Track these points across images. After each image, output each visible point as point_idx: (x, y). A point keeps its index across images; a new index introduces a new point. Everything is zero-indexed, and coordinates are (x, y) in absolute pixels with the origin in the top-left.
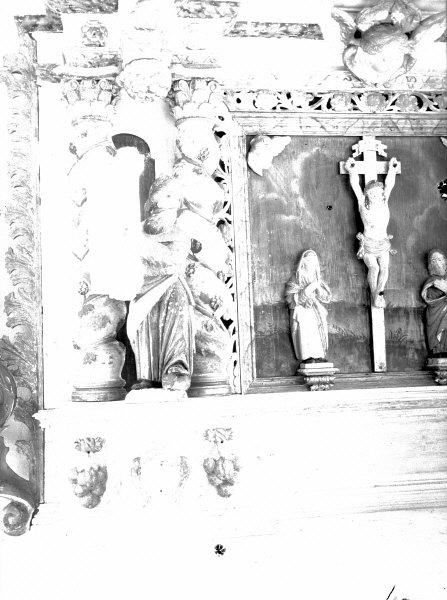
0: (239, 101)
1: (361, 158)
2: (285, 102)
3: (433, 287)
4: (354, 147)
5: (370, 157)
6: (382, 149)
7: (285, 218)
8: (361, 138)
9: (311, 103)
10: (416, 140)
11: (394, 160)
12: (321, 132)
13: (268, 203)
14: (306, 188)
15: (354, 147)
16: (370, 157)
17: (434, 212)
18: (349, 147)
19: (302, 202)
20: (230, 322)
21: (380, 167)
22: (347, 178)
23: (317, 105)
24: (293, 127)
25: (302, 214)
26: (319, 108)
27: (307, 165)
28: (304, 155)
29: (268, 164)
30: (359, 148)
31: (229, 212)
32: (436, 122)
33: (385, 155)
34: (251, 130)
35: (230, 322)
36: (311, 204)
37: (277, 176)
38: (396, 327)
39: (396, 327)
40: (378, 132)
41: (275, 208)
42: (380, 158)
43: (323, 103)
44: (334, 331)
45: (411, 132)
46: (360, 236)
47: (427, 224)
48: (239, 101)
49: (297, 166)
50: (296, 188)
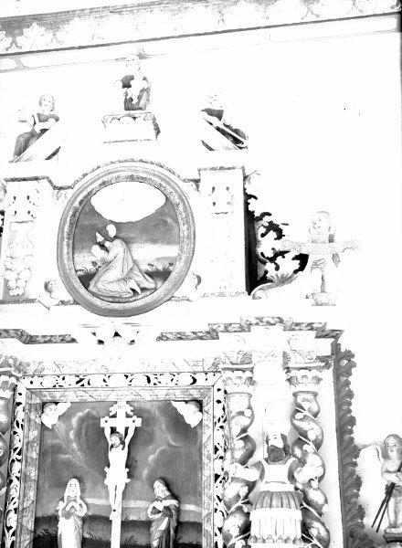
0: (32, 382)
1: (114, 416)
2: (61, 383)
3: (154, 508)
4: (111, 409)
5: (121, 415)
6: (129, 409)
7: (63, 456)
8: (116, 402)
9: (77, 383)
11: (135, 417)
12: (90, 399)
13: (53, 446)
14: (78, 434)
15: (111, 409)
16: (121, 415)
17: (163, 452)
19: (74, 445)
20: (11, 528)
21: (129, 422)
22: (103, 429)
23: (81, 384)
24: (72, 397)
25: (75, 453)
27: (82, 420)
29: (55, 421)
30: (113, 410)
31: (19, 454)
33: (131, 414)
34: (45, 399)
35: (11, 528)
36: (80, 450)
37: (62, 427)
38: (129, 535)
39: (129, 535)
40: (129, 399)
41: (57, 450)
42: (128, 416)
43: (85, 382)
44: (87, 536)
45: (150, 398)
47: (157, 461)
48: (32, 382)
49: (74, 421)
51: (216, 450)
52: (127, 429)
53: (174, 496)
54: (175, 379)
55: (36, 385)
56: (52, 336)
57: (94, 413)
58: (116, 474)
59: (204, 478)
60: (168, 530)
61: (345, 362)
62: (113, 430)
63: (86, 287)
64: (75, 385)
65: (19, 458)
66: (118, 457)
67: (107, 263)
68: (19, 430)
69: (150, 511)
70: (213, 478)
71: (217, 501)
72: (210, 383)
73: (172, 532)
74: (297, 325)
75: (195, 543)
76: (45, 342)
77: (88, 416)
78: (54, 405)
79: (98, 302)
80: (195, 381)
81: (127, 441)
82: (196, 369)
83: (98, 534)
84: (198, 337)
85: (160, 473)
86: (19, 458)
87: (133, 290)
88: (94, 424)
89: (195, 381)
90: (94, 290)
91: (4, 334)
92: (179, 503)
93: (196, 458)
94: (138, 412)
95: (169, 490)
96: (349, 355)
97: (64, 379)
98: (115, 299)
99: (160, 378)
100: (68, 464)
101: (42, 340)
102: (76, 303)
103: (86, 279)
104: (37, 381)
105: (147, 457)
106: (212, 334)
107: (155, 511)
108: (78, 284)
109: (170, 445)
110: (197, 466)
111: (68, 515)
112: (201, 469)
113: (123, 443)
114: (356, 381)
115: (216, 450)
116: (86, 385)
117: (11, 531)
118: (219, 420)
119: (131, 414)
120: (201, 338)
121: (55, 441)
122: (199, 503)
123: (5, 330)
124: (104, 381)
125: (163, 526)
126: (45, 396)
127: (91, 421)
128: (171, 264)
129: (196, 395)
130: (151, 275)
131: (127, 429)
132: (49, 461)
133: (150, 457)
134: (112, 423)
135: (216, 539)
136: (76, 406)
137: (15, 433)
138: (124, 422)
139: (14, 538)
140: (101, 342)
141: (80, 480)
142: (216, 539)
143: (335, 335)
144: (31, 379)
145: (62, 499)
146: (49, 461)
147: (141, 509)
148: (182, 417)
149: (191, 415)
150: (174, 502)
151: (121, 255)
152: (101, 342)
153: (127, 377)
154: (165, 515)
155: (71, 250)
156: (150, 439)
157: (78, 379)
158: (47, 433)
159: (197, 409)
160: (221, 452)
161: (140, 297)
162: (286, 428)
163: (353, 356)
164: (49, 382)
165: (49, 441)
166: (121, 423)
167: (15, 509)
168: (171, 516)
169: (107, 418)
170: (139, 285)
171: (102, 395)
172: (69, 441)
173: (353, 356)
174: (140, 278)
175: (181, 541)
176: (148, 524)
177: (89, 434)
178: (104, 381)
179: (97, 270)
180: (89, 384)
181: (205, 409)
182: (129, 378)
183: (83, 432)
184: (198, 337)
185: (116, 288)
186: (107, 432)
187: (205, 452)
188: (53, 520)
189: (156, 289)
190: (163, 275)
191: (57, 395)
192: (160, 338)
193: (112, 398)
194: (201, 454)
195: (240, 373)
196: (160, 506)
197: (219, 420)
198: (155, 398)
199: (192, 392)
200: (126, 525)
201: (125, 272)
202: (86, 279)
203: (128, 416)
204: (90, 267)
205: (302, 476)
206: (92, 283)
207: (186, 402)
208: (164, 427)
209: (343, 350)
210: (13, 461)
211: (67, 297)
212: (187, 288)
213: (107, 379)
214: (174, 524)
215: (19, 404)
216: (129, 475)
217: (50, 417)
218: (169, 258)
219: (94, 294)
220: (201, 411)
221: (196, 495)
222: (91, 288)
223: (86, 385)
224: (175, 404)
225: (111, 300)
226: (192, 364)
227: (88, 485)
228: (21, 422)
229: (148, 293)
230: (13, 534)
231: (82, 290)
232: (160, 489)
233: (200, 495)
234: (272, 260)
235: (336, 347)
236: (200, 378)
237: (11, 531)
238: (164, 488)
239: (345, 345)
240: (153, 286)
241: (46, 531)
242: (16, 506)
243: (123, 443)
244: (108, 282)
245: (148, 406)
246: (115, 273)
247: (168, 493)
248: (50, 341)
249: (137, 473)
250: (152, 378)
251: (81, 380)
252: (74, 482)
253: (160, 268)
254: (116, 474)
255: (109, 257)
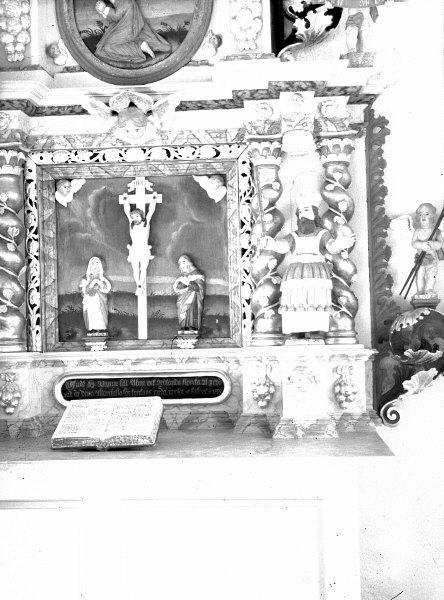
0: (41, 158)
1: (133, 193)
2: (74, 158)
3: (180, 283)
4: (129, 185)
5: (140, 191)
6: (148, 185)
7: (83, 235)
8: (134, 178)
9: (91, 158)
10: (175, 178)
11: (155, 194)
12: (106, 175)
14: (96, 212)
15: (129, 185)
16: (140, 191)
17: (186, 228)
18: (123, 183)
19: (93, 224)
20: (35, 305)
21: (149, 199)
22: (122, 206)
24: (87, 173)
25: (95, 232)
26: (98, 161)
27: (99, 198)
28: (96, 191)
29: (70, 198)
30: (131, 186)
31: (36, 233)
32: (186, 166)
33: (151, 190)
34: (57, 176)
35: (35, 305)
37: (78, 207)
39: (157, 309)
40: (147, 174)
41: (73, 229)
42: (147, 192)
43: (99, 157)
44: (113, 311)
46: (128, 246)
47: (181, 237)
48: (41, 158)
49: (91, 198)
50: (89, 213)
51: (243, 224)
52: (147, 206)
53: (200, 271)
54: (197, 152)
55: (47, 160)
56: (60, 107)
57: (111, 189)
58: (139, 251)
59: (230, 253)
60: (195, 303)
61: (377, 130)
62: (133, 208)
63: (93, 50)
64: (88, 161)
65: (36, 237)
66: (140, 234)
67: (114, 22)
68: (33, 209)
69: (175, 285)
70: (240, 252)
71: (245, 274)
72: (234, 155)
73: (199, 305)
74: (330, 89)
75: (222, 314)
76: (53, 114)
77: (105, 193)
78: (67, 184)
79: (104, 66)
80: (218, 154)
81: (149, 218)
82: (219, 141)
83: (124, 308)
84: (221, 105)
85: (184, 249)
86: (36, 237)
87: (146, 54)
88: (112, 202)
89: (218, 154)
90: (102, 55)
91: (7, 105)
92: (206, 277)
93: (221, 233)
94: (158, 188)
95: (194, 265)
96: (383, 122)
97: (76, 154)
98: (126, 65)
99: (181, 152)
100: (88, 243)
101: (50, 112)
102: (83, 70)
103: (92, 42)
104: (47, 156)
105: (170, 235)
106: (236, 102)
107: (182, 286)
108: (83, 48)
109: (193, 221)
110: (222, 242)
111: (92, 292)
112: (227, 244)
113: (144, 220)
114: (390, 149)
115: (243, 224)
116: (101, 161)
117: (36, 309)
118: (245, 194)
119: (151, 190)
120: (224, 107)
121: (72, 220)
122: (225, 277)
123: (8, 101)
124: (121, 155)
125: (190, 300)
126: (57, 173)
127: (108, 199)
128: (187, 23)
129: (219, 167)
130: (165, 36)
131: (147, 206)
132: (67, 239)
133: (173, 233)
134: (132, 199)
135: (244, 310)
136: (91, 183)
137: (29, 212)
138: (141, 197)
139: (39, 315)
140: (114, 113)
141: (102, 259)
142: (244, 310)
143: (369, 99)
144: (40, 155)
145: (85, 277)
146: (67, 239)
147: (166, 284)
148: (205, 191)
149: (213, 189)
150: (200, 277)
151: (129, 12)
152: (114, 113)
153: (145, 151)
154: (191, 289)
155: (72, 5)
156: (172, 215)
157: (91, 154)
158: (62, 211)
159: (221, 183)
160: (247, 227)
161: (153, 62)
162: (317, 200)
163: (387, 122)
164: (60, 158)
165: (66, 219)
166: (140, 199)
167: (37, 288)
168: (197, 290)
169: (125, 195)
170: (151, 48)
171: (116, 171)
172: (87, 220)
173: (387, 122)
174: (152, 39)
175: (208, 313)
176: (174, 299)
177: (107, 211)
178: (121, 155)
179: (104, 31)
180: (104, 159)
181: (230, 183)
182: (148, 152)
183: (101, 209)
184: (221, 105)
185: (125, 51)
186: (127, 209)
187: (230, 227)
188: (78, 297)
189: (171, 53)
190: (178, 36)
191: (71, 170)
192: (179, 109)
193: (129, 173)
194: (226, 229)
195: (267, 144)
196: (186, 281)
197: (245, 194)
198: (175, 172)
199: (214, 165)
200: (152, 300)
201: (136, 34)
202: (92, 42)
203: (147, 192)
204: (95, 28)
205: (333, 247)
206: (99, 46)
207: (209, 176)
208: (186, 203)
209: (376, 117)
210: (30, 240)
211: (72, 62)
212: (205, 52)
213: (122, 153)
214: (201, 297)
215: (30, 181)
216: (153, 252)
217: (64, 196)
218: (185, 15)
219: (102, 59)
220: (225, 185)
221: (222, 268)
222: (98, 52)
223: (101, 161)
224: (196, 179)
225: (121, 66)
226: (214, 135)
227: (110, 263)
228: (34, 200)
229: (163, 57)
230: (38, 312)
231: (89, 55)
232: (185, 264)
233: (227, 269)
234: (302, 15)
235: (369, 113)
236: (224, 152)
237: (36, 309)
238: (189, 264)
239: (379, 109)
240: (167, 49)
241: (71, 308)
242: (38, 284)
243: (144, 220)
244: (116, 44)
245: (168, 182)
246: (124, 33)
247: (193, 269)
248: (57, 113)
249: (158, 250)
250: (172, 151)
251: (95, 155)
252: (96, 260)
253: (175, 28)
254: (139, 251)
255: (118, 14)
